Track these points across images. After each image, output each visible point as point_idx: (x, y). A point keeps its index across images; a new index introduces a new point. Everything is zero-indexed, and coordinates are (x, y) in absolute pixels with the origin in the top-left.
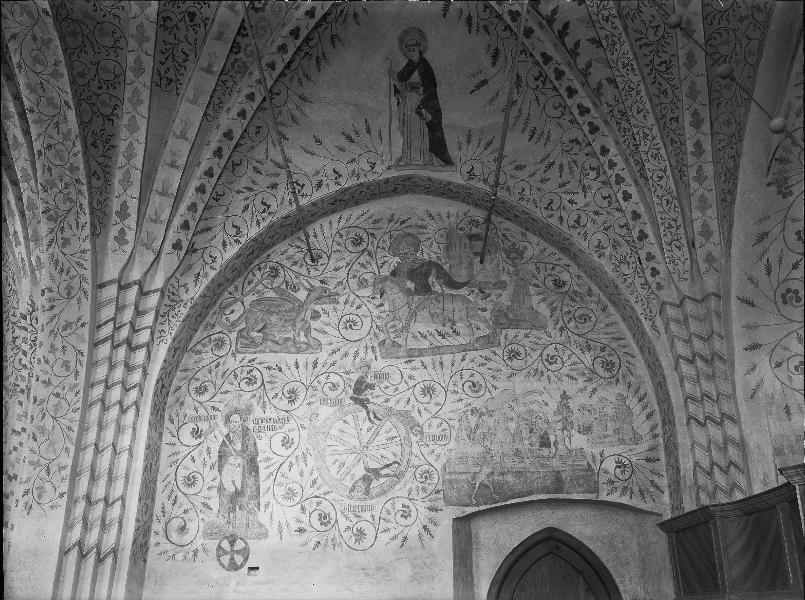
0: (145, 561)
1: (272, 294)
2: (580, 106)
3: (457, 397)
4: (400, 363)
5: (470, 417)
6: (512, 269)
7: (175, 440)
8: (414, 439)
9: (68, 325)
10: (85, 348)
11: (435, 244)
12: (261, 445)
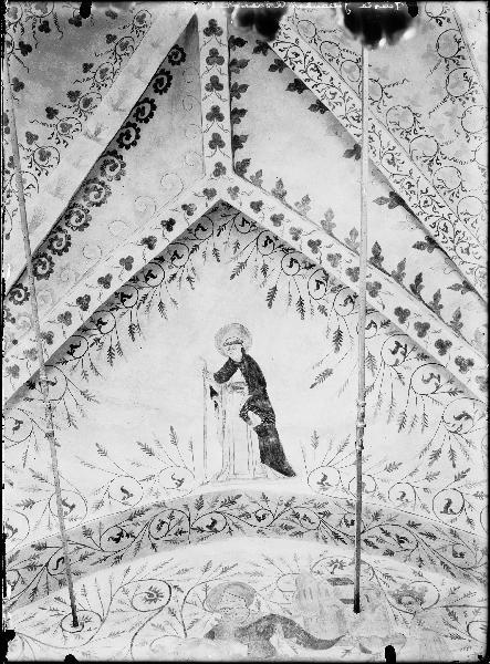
2: (459, 362)
6: (409, 617)
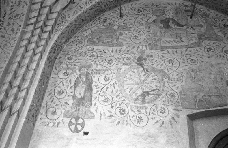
0: (34, 125)
1: (103, 27)
3: (185, 64)
4: (158, 51)
5: (191, 72)
6: (204, 21)
7: (56, 76)
8: (165, 80)
9: (17, 15)
10: (22, 24)
11: (171, 12)
12: (94, 79)
